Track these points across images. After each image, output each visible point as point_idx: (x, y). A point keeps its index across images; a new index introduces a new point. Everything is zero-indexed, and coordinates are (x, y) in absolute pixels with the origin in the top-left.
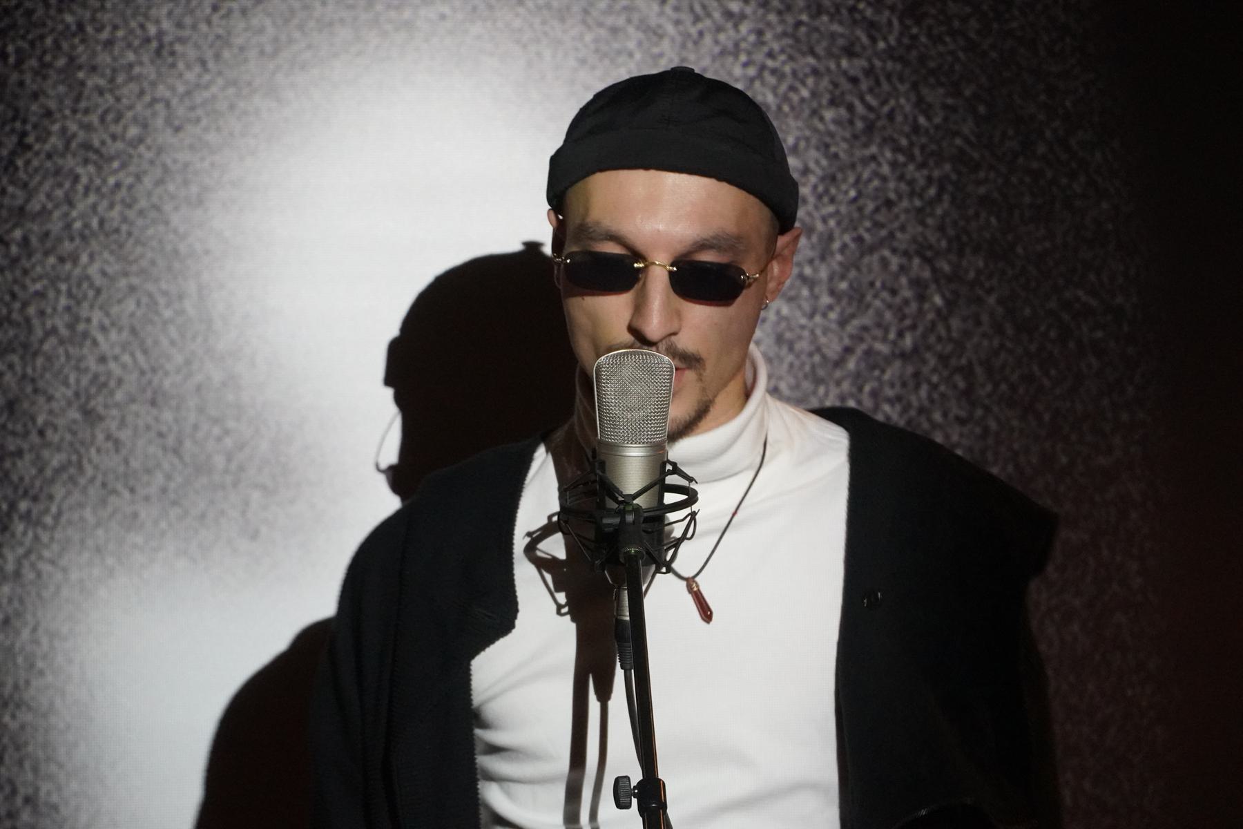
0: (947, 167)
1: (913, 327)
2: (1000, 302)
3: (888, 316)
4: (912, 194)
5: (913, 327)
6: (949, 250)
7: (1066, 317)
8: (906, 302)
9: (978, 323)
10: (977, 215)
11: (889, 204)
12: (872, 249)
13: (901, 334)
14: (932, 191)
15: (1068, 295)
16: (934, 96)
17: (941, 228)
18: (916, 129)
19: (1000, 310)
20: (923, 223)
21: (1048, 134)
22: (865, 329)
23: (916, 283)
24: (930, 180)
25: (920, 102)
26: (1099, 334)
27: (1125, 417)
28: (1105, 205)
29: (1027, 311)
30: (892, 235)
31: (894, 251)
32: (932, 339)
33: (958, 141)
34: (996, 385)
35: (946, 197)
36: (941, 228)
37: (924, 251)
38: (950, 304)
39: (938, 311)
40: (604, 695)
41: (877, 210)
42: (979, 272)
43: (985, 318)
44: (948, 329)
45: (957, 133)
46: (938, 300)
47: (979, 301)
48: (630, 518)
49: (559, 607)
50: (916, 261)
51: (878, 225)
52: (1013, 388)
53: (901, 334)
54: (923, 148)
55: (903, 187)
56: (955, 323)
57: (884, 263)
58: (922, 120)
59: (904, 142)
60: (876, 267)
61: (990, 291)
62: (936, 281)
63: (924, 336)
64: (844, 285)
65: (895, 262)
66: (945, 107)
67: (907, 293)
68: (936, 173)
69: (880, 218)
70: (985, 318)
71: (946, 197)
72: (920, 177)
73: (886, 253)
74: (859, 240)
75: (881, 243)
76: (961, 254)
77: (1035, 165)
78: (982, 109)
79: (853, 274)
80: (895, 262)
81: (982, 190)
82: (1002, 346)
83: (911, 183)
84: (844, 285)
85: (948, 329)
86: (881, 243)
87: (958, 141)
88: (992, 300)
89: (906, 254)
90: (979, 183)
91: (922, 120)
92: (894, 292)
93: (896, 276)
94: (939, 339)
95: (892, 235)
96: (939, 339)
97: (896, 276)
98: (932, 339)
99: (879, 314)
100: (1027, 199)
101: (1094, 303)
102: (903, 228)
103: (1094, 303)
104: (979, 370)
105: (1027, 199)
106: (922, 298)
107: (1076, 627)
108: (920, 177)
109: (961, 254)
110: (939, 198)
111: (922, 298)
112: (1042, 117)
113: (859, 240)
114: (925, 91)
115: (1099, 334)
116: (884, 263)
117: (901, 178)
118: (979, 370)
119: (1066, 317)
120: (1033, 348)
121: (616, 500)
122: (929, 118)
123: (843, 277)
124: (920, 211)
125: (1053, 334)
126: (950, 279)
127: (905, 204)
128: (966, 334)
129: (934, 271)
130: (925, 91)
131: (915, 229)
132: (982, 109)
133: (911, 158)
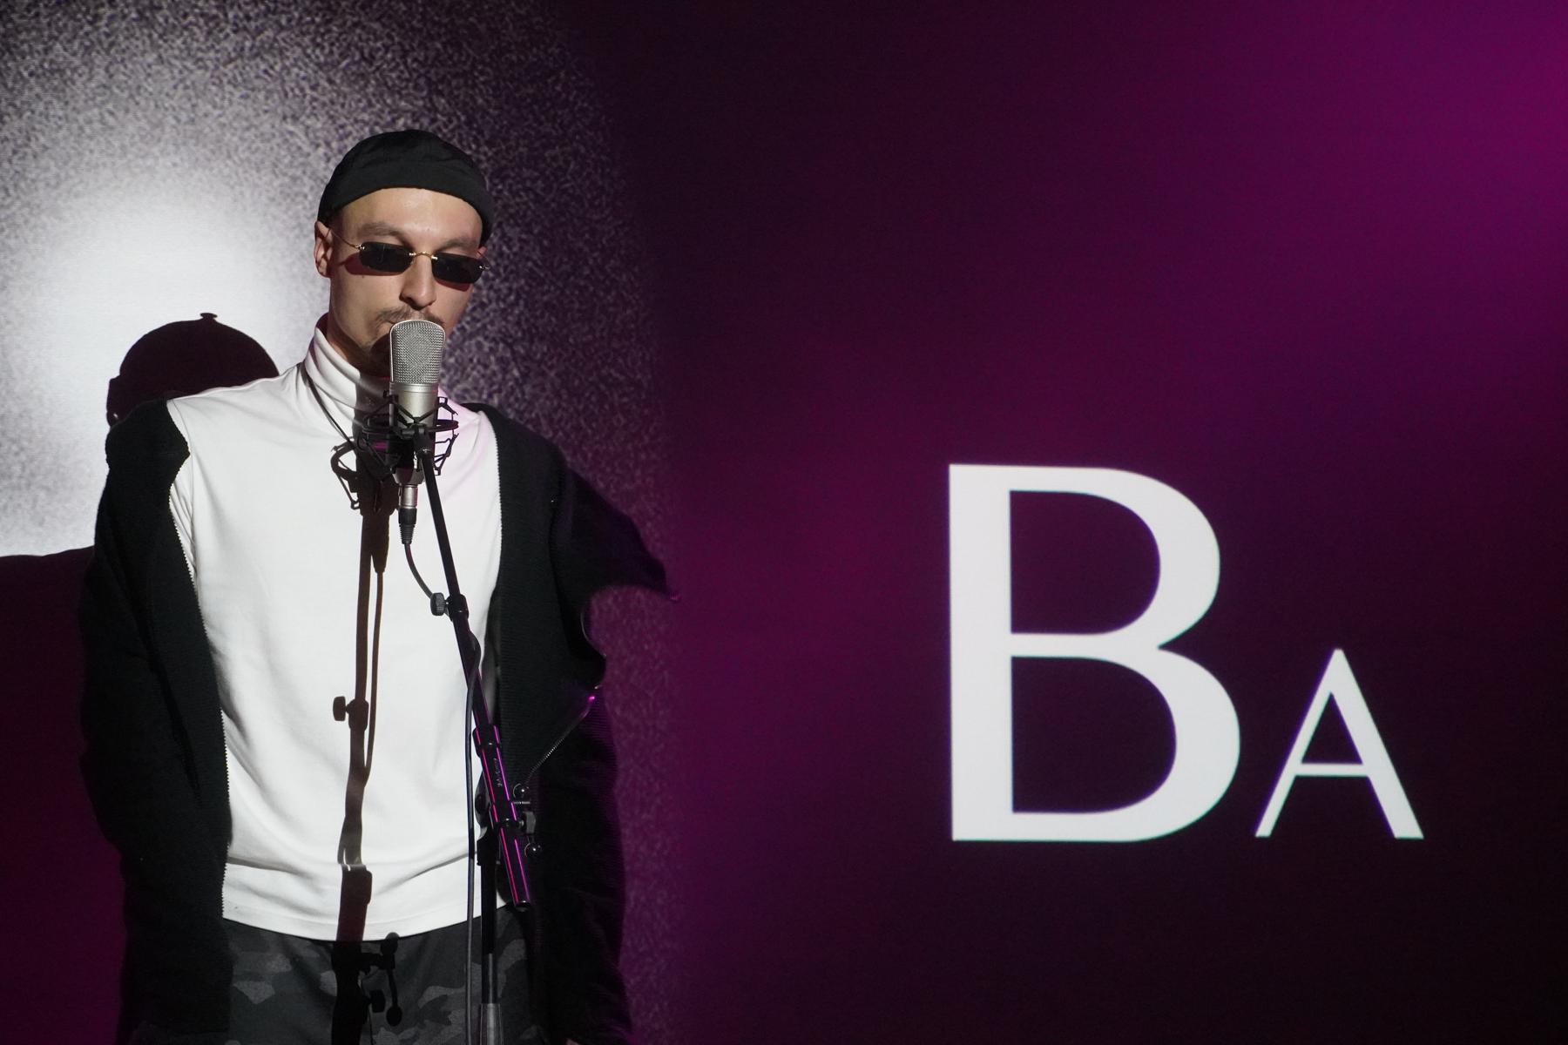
0: (523, 282)
1: (499, 391)
2: (557, 375)
3: (482, 382)
4: (498, 299)
5: (499, 391)
6: (523, 339)
7: (602, 387)
8: (494, 373)
9: (544, 390)
10: (542, 316)
11: (483, 305)
12: (471, 336)
13: (490, 395)
14: (512, 298)
15: (604, 372)
16: (512, 232)
17: (518, 323)
18: (501, 254)
19: (558, 381)
20: (505, 319)
21: (591, 262)
22: (466, 391)
23: (500, 360)
24: (510, 289)
25: (504, 235)
26: (625, 400)
27: (643, 456)
28: (629, 312)
29: (577, 382)
30: (484, 326)
31: (486, 338)
32: (512, 399)
33: (530, 264)
34: (556, 432)
35: (522, 302)
36: (518, 323)
37: (505, 338)
38: (524, 376)
39: (516, 380)
40: (380, 568)
41: (474, 309)
42: (544, 354)
43: (548, 386)
44: (523, 393)
45: (528, 259)
46: (516, 373)
47: (543, 374)
48: (421, 431)
49: (353, 502)
50: (501, 345)
51: (475, 320)
52: (567, 435)
53: (490, 395)
54: (506, 268)
55: (492, 294)
56: (528, 389)
57: (479, 346)
58: (504, 248)
59: (493, 263)
60: (474, 349)
61: (551, 368)
62: (514, 359)
63: (507, 397)
64: (452, 360)
65: (487, 345)
66: (520, 240)
67: (494, 367)
68: (515, 286)
69: (477, 315)
70: (548, 386)
71: (522, 302)
72: (504, 287)
73: (480, 339)
74: (462, 329)
75: (478, 332)
76: (532, 342)
77: (582, 283)
78: (546, 243)
79: (458, 353)
80: (487, 345)
81: (545, 298)
82: (559, 406)
83: (498, 291)
84: (452, 360)
85: (523, 393)
86: (478, 332)
87: (530, 264)
88: (552, 374)
89: (494, 339)
90: (543, 294)
91: (504, 248)
92: (486, 367)
93: (488, 355)
94: (517, 399)
95: (484, 326)
96: (517, 399)
97: (488, 355)
98: (512, 399)
99: (476, 381)
100: (577, 306)
101: (622, 378)
102: (492, 323)
103: (622, 378)
104: (543, 421)
105: (577, 306)
106: (505, 371)
107: (610, 601)
108: (504, 287)
109: (532, 342)
110: (516, 303)
111: (505, 371)
112: (586, 249)
113: (462, 329)
114: (507, 229)
115: (625, 400)
116: (479, 346)
117: (491, 288)
118: (543, 421)
119: (602, 387)
120: (581, 407)
121: (404, 422)
122: (510, 248)
123: (451, 355)
124: (504, 310)
125: (594, 399)
126: (524, 359)
127: (494, 305)
128: (535, 397)
129: (513, 352)
130: (507, 229)
131: (500, 324)
132: (546, 243)
133: (498, 274)
